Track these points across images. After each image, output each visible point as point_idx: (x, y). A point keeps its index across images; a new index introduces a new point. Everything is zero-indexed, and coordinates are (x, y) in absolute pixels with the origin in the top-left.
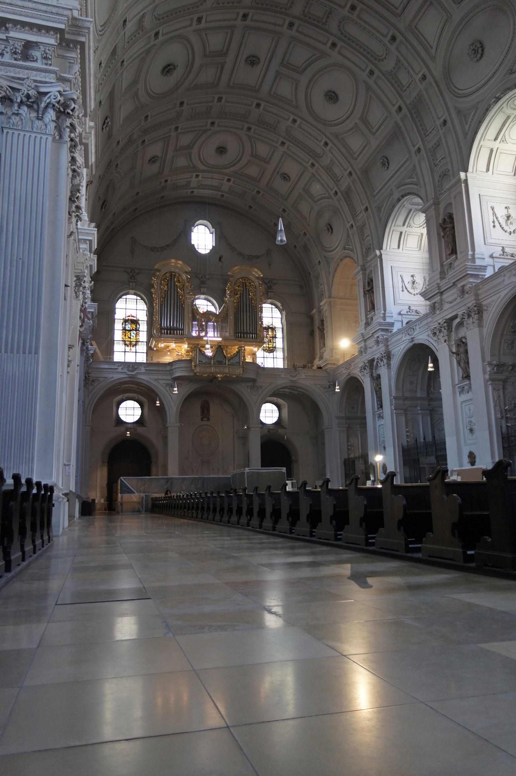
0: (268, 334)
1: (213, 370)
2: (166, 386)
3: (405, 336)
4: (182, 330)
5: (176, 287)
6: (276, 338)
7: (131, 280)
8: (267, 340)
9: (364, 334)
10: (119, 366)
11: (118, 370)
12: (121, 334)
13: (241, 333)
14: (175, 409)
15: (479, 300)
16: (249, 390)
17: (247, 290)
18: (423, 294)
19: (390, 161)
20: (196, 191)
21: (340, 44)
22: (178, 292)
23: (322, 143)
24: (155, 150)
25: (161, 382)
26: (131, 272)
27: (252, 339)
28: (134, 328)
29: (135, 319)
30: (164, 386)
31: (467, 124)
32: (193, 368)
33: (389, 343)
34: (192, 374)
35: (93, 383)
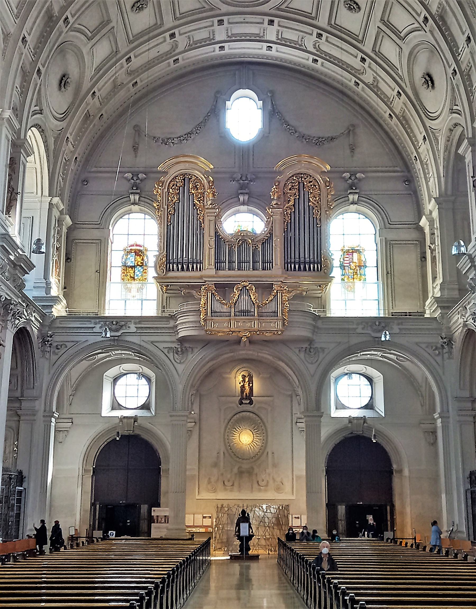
0: (353, 262)
2: (168, 352)
6: (365, 266)
7: (132, 191)
8: (352, 271)
9: (473, 256)
10: (96, 323)
11: (95, 330)
12: (120, 273)
14: (180, 387)
16: (302, 355)
22: (194, 205)
25: (161, 346)
28: (139, 263)
29: (142, 249)
30: (166, 351)
34: (203, 333)
35: (57, 351)
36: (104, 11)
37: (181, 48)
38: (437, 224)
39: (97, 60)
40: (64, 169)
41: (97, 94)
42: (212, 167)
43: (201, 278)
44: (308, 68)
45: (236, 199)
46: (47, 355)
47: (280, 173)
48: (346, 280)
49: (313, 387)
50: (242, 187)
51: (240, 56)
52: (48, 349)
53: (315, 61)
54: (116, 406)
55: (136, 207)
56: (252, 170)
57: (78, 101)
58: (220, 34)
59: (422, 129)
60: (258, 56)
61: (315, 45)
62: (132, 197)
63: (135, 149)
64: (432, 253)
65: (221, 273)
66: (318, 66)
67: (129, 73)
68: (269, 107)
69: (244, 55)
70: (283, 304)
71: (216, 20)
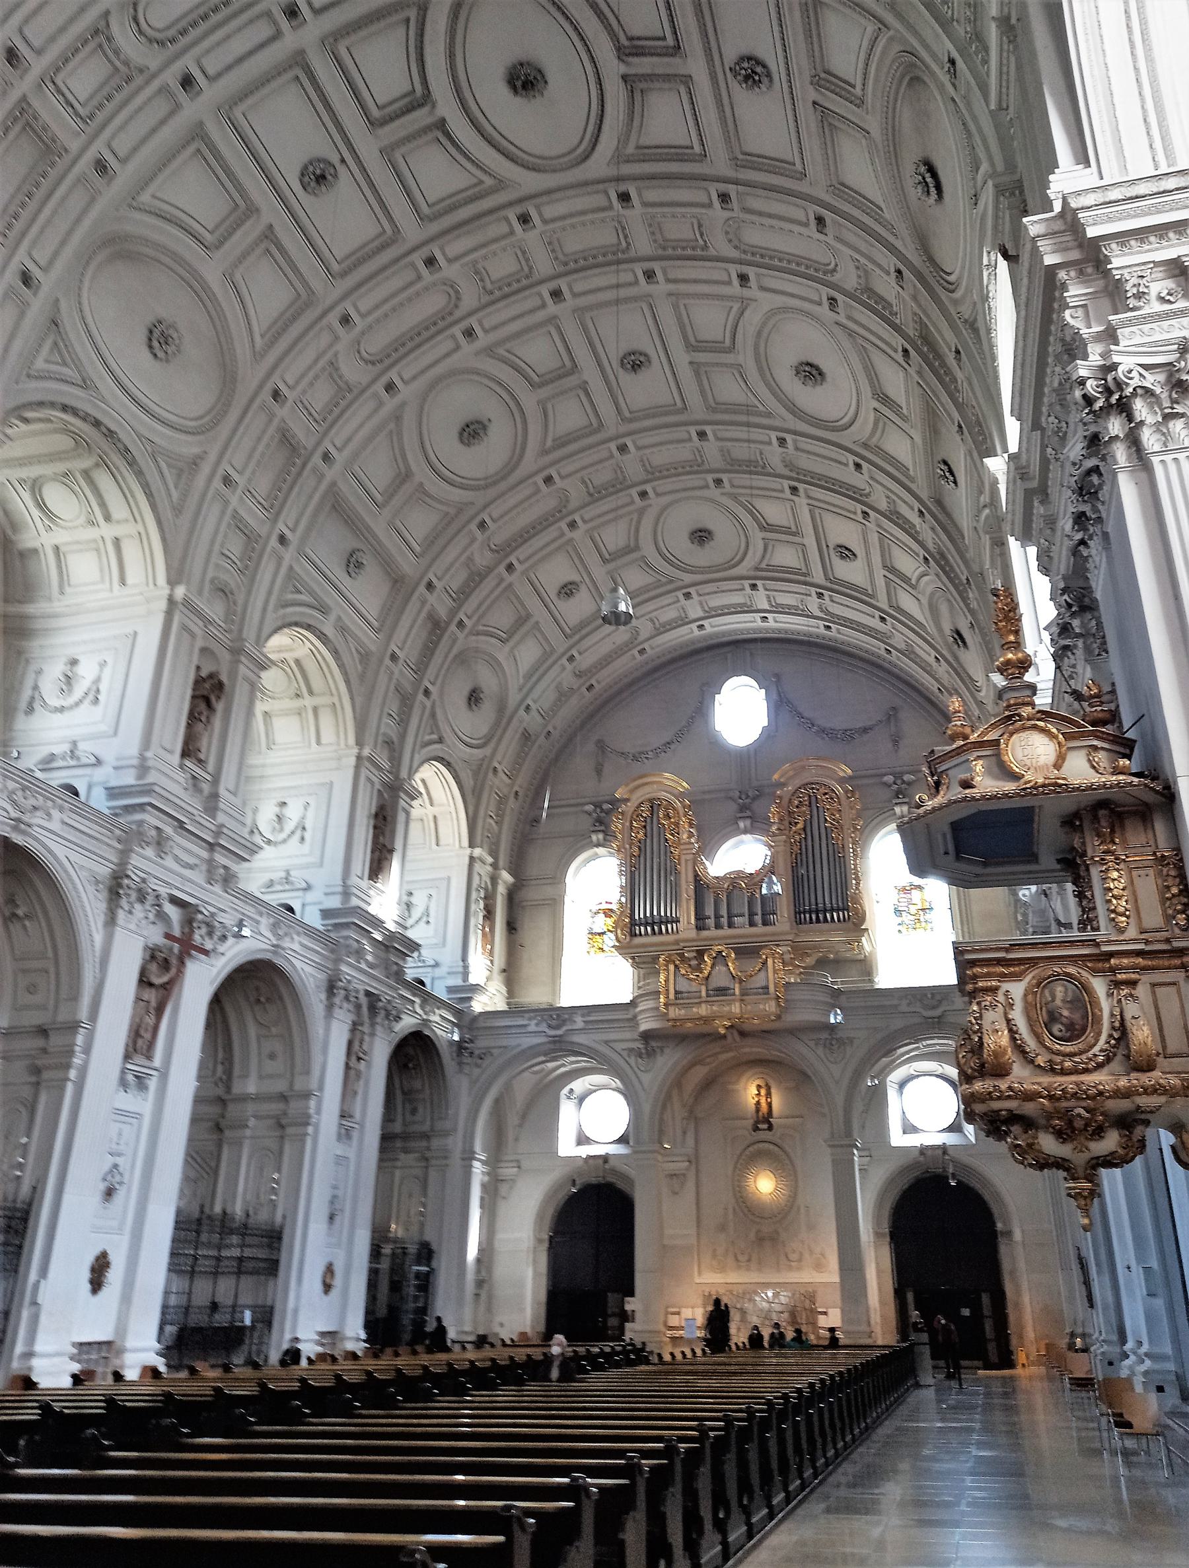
1: (703, 1010)
13: (810, 912)
17: (821, 810)
20: (705, 623)
24: (556, 572)
26: (595, 811)
27: (833, 925)
36: (517, 605)
37: (644, 634)
40: (499, 809)
43: (677, 942)
44: (824, 638)
45: (735, 827)
47: (784, 785)
50: (743, 808)
51: (730, 633)
55: (601, 850)
56: (755, 783)
57: (505, 720)
58: (694, 611)
60: (748, 631)
62: (594, 837)
63: (599, 771)
65: (705, 933)
66: (833, 633)
67: (579, 675)
68: (775, 696)
69: (735, 631)
71: (680, 594)
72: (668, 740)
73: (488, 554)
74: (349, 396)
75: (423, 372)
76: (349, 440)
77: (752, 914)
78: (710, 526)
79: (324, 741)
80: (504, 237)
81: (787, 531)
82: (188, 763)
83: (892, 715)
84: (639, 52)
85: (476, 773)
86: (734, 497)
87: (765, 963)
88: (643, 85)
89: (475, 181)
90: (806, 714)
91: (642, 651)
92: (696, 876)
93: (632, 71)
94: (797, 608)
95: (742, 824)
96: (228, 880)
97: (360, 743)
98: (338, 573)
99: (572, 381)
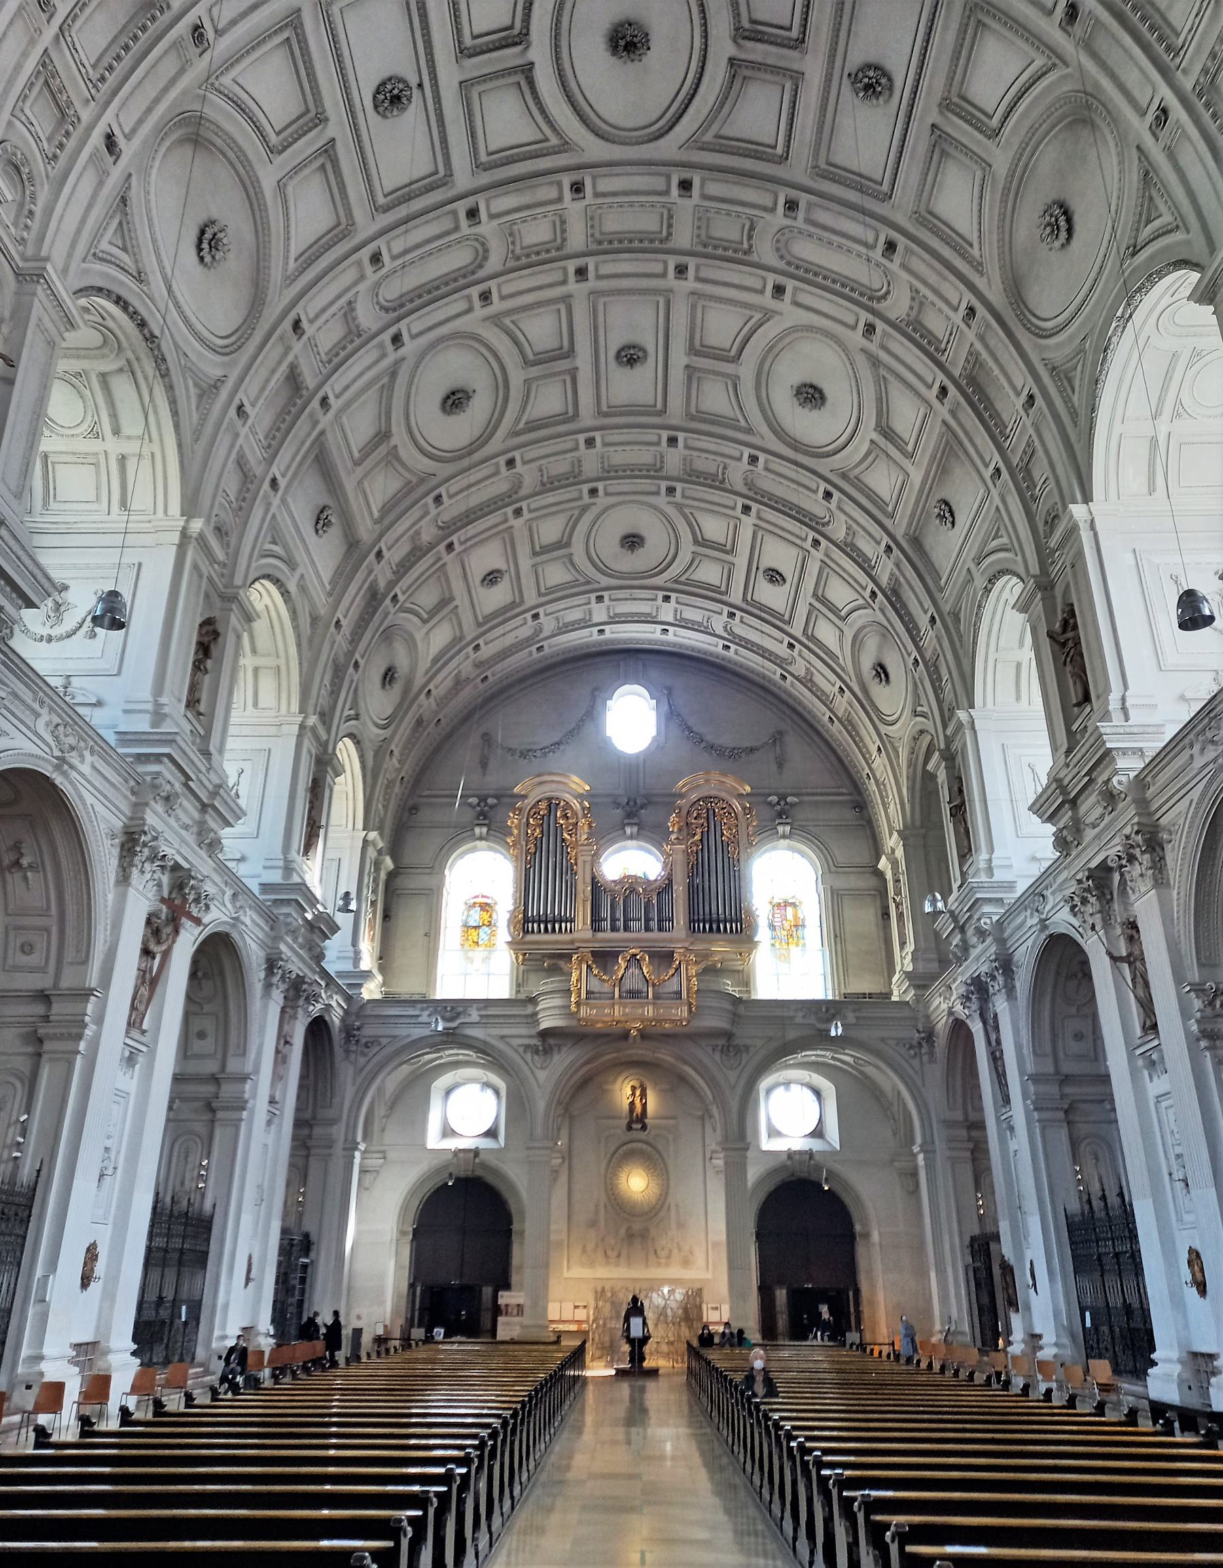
1: (618, 1012)
2: (525, 1052)
3: (1032, 915)
4: (572, 921)
5: (559, 829)
6: (804, 926)
10: (422, 1010)
11: (421, 1020)
14: (541, 1105)
15: (1151, 814)
16: (717, 1056)
18: (1035, 808)
19: (954, 508)
20: (607, 628)
21: (790, 284)
22: (563, 840)
23: (821, 493)
24: (488, 557)
26: (478, 805)
29: (489, 901)
30: (521, 1050)
31: (1074, 392)
32: (573, 1008)
33: (1006, 935)
34: (574, 1023)
35: (366, 1050)
36: (445, 586)
38: (903, 866)
39: (434, 650)
40: (386, 793)
41: (434, 692)
42: (588, 788)
43: (572, 942)
44: (717, 657)
45: (621, 832)
46: (353, 1056)
47: (681, 796)
48: (777, 945)
49: (734, 1104)
50: (630, 815)
51: (625, 641)
52: (354, 1048)
53: (727, 647)
54: (448, 1132)
57: (407, 703)
58: (599, 613)
59: (875, 737)
60: (650, 642)
61: (725, 627)
62: (477, 830)
63: (484, 764)
64: (897, 907)
65: (600, 935)
67: (478, 665)
68: (666, 707)
69: (631, 640)
70: (689, 980)
71: (593, 596)
72: (556, 739)
73: (434, 530)
74: (357, 341)
75: (430, 329)
76: (347, 387)
77: (647, 920)
78: (644, 533)
79: (261, 705)
80: (551, 202)
81: (720, 548)
82: (189, 715)
83: (778, 738)
84: (758, 38)
85: (377, 753)
86: (679, 507)
87: (678, 968)
88: (747, 73)
89: (540, 136)
90: (695, 729)
91: (540, 649)
92: (593, 878)
93: (743, 56)
94: (700, 624)
95: (628, 830)
96: (213, 846)
97: (302, 710)
98: (308, 529)
99: (564, 365)
